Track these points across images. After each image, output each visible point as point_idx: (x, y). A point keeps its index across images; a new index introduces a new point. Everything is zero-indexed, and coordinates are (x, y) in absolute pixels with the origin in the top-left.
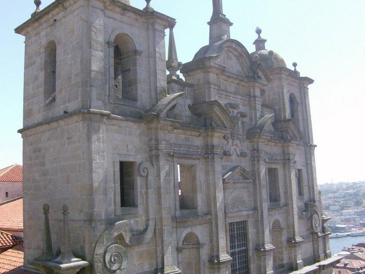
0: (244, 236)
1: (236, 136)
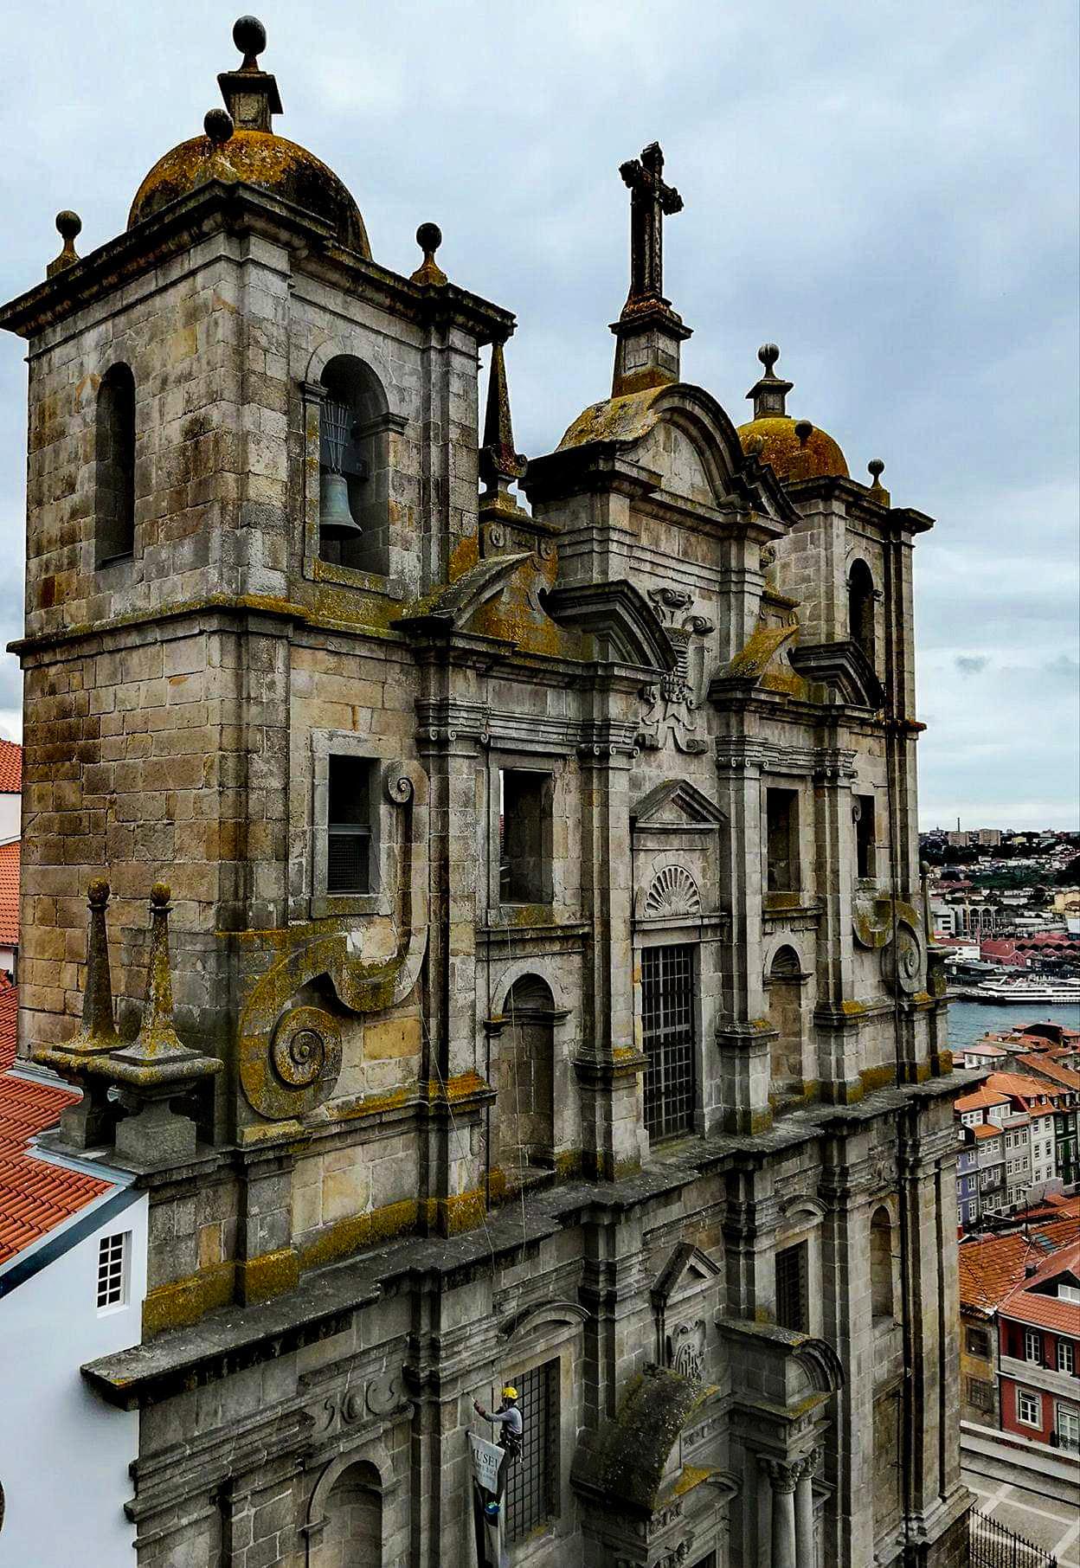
0: (686, 993)
1: (677, 689)
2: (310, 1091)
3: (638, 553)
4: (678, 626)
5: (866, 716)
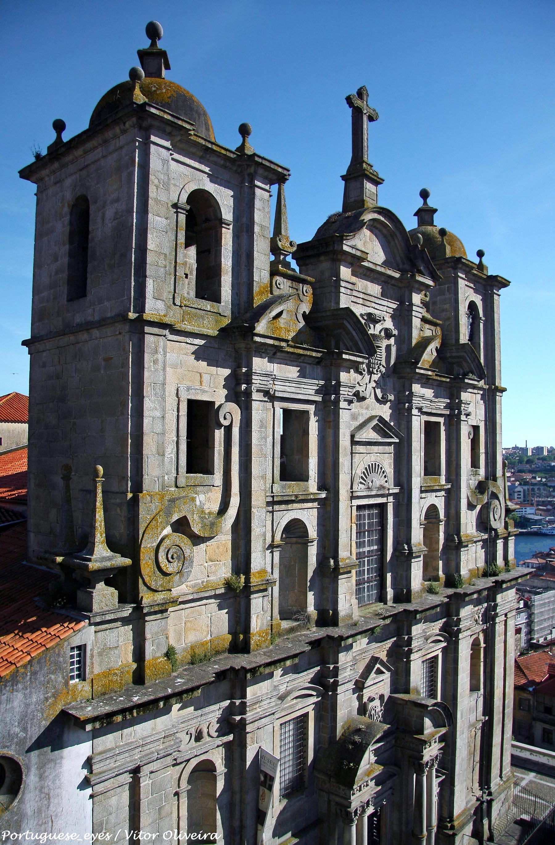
2: (178, 576)
3: (355, 293)
4: (377, 332)
5: (476, 383)
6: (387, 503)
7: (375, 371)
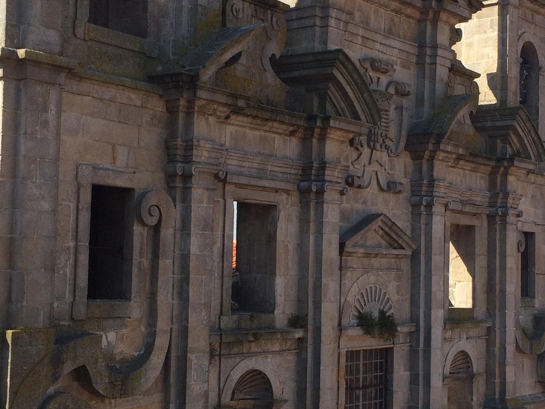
1: (380, 140)
3: (351, 28)
4: (382, 88)
6: (392, 348)
7: (378, 147)
